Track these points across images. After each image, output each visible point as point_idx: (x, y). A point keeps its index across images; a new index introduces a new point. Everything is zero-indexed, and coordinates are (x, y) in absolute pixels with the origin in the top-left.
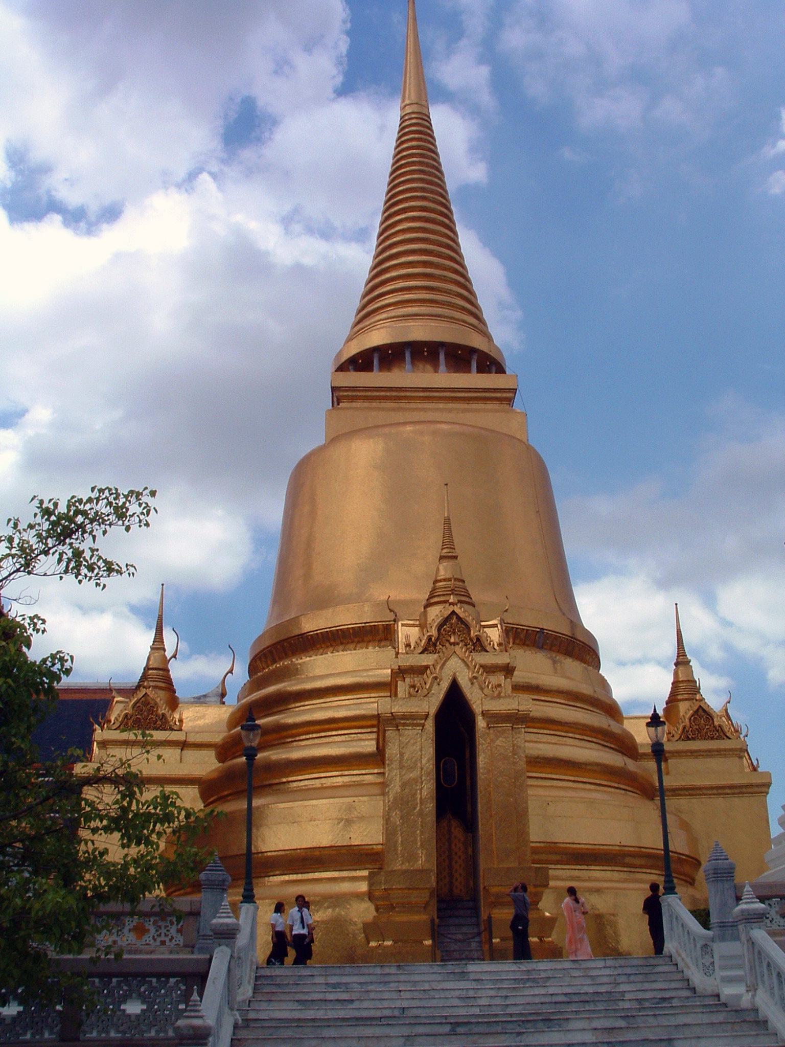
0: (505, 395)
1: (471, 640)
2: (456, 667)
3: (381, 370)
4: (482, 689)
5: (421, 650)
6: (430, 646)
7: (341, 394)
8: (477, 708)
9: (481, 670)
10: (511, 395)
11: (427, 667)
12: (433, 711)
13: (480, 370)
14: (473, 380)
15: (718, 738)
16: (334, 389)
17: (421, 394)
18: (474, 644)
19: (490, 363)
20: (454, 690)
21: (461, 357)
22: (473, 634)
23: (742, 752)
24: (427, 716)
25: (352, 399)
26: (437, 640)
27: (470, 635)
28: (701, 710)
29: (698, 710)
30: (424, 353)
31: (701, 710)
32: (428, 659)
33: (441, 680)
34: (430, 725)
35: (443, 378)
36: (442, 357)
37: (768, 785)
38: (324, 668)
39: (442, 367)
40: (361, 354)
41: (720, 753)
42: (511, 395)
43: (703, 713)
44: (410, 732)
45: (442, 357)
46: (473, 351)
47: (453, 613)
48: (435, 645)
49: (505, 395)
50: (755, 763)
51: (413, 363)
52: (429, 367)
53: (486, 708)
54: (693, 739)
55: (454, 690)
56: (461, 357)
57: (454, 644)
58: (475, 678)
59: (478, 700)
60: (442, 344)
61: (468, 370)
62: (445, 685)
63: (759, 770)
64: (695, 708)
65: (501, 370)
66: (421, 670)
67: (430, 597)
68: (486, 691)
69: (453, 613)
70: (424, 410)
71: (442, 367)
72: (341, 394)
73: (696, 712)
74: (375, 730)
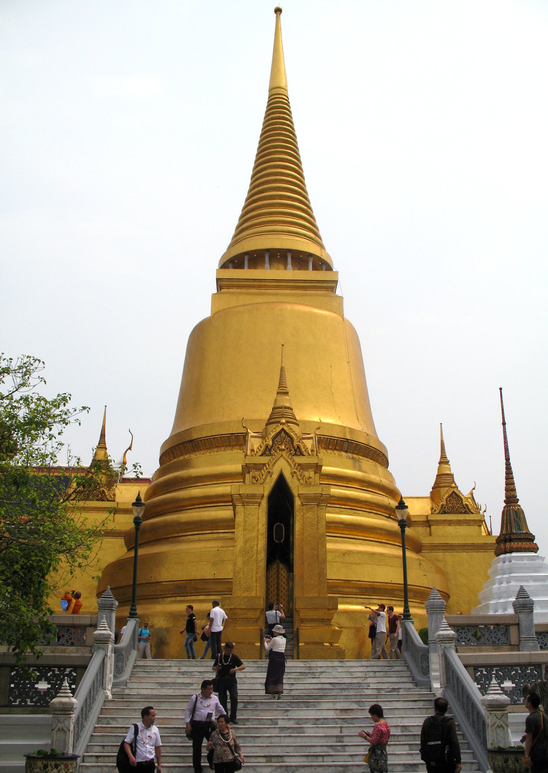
1: (294, 447)
2: (282, 465)
3: (249, 268)
4: (299, 480)
5: (260, 453)
6: (267, 451)
7: (222, 283)
8: (295, 492)
9: (299, 467)
10: (334, 285)
11: (264, 465)
12: (266, 493)
13: (315, 268)
14: (310, 274)
16: (218, 280)
17: (274, 284)
18: (295, 450)
20: (281, 479)
24: (263, 496)
25: (229, 287)
26: (272, 447)
27: (293, 444)
32: (264, 460)
33: (272, 473)
34: (264, 503)
35: (290, 273)
39: (290, 266)
40: (236, 257)
42: (334, 285)
44: (252, 508)
47: (283, 429)
48: (270, 450)
49: (329, 285)
51: (270, 264)
52: (281, 266)
53: (300, 492)
55: (281, 479)
56: (301, 259)
58: (295, 473)
60: (290, 251)
61: (307, 269)
62: (275, 476)
65: (329, 268)
66: (259, 467)
67: (270, 419)
68: (301, 481)
69: (283, 429)
70: (276, 294)
71: (290, 266)
72: (222, 283)
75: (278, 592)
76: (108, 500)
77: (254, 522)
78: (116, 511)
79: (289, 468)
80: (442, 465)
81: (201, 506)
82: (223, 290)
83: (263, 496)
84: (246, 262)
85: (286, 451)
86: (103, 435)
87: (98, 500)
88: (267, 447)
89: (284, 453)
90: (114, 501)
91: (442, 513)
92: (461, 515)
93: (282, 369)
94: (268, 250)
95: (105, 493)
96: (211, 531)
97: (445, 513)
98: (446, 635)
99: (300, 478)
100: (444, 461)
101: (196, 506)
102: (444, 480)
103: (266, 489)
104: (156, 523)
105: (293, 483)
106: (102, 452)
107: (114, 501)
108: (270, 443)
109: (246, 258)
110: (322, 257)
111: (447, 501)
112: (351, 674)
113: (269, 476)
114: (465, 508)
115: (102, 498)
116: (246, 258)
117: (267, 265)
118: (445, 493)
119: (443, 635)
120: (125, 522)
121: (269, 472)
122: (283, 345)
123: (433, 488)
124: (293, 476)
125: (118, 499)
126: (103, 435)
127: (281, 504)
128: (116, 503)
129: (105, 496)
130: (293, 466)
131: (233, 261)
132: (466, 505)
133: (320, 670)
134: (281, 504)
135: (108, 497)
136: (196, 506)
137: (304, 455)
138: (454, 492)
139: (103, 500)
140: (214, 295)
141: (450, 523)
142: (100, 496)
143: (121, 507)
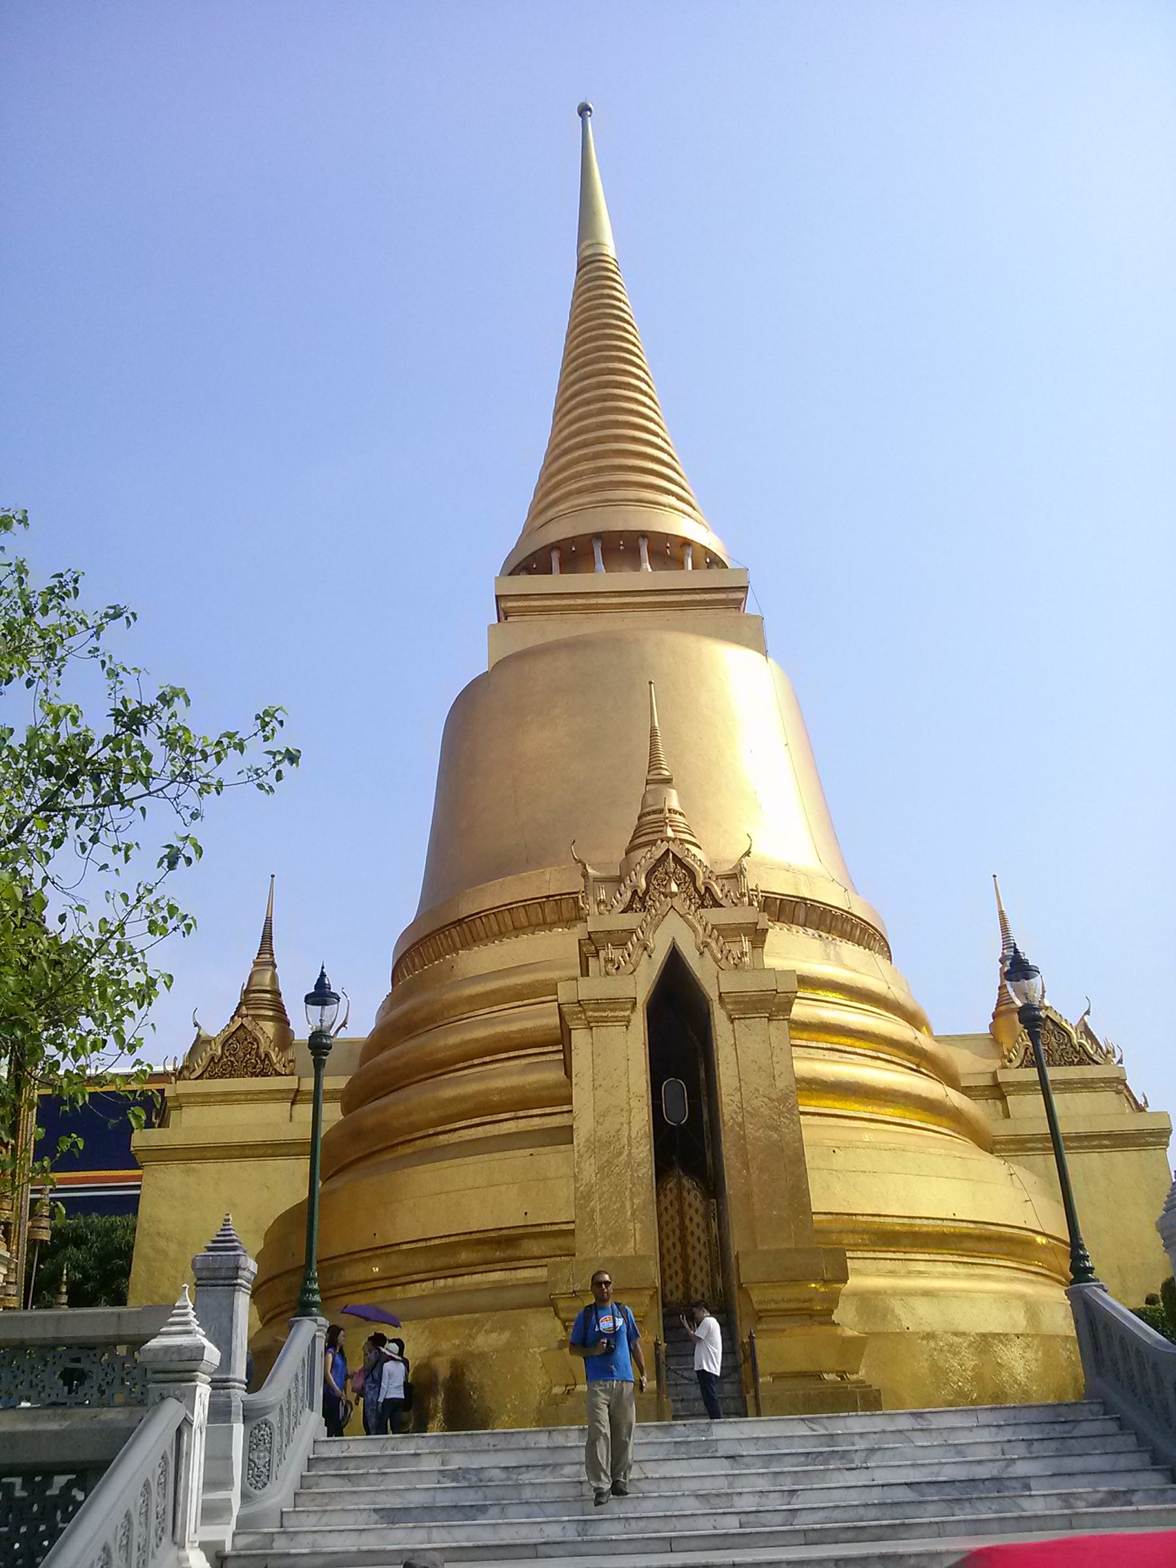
1: (696, 890)
2: (674, 930)
4: (717, 961)
7: (509, 604)
11: (632, 932)
15: (1081, 1063)
18: (702, 897)
20: (675, 960)
23: (1118, 1085)
25: (524, 612)
34: (639, 1021)
37: (1167, 1132)
38: (483, 961)
41: (1088, 1085)
42: (740, 595)
48: (642, 900)
50: (1141, 1101)
55: (675, 960)
62: (660, 956)
63: (1148, 1110)
66: (620, 939)
67: (634, 838)
68: (723, 964)
72: (509, 604)
74: (561, 1047)
75: (684, 1247)
77: (615, 1071)
81: (487, 1059)
82: (509, 619)
84: (555, 564)
86: (267, 938)
87: (254, 1075)
88: (635, 892)
89: (676, 902)
94: (598, 536)
96: (512, 1115)
101: (476, 1061)
103: (642, 982)
105: (702, 969)
109: (555, 556)
112: (959, 1453)
115: (263, 1068)
116: (555, 556)
117: (600, 566)
126: (267, 938)
127: (679, 1022)
129: (271, 1064)
130: (700, 929)
131: (530, 563)
133: (861, 1444)
134: (679, 1022)
135: (278, 1067)
136: (476, 1061)
137: (722, 906)
139: (266, 1075)
142: (260, 1065)
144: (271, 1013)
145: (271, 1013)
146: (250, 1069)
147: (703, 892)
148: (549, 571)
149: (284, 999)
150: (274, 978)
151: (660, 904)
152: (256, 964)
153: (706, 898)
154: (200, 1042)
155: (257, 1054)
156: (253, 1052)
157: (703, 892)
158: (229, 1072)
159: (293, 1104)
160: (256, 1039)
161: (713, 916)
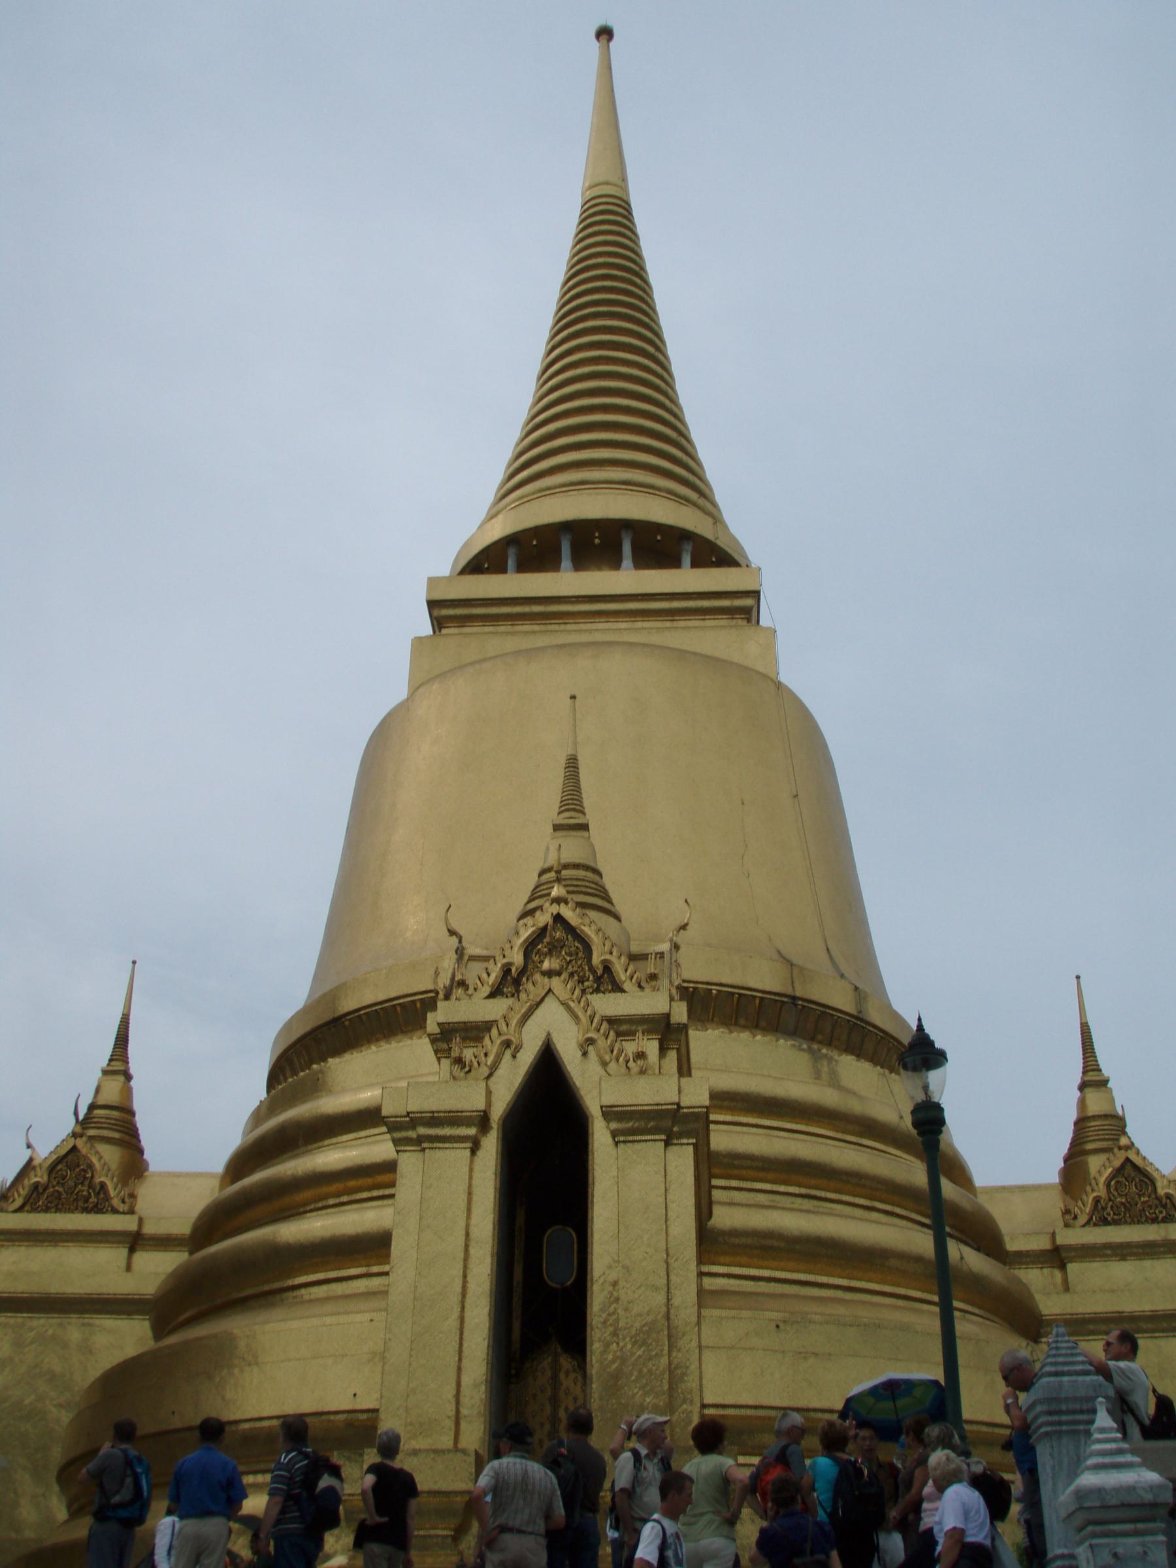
0: (738, 603)
1: (592, 970)
2: (555, 1021)
4: (604, 1064)
5: (486, 990)
8: (593, 1107)
9: (605, 1025)
16: (432, 604)
18: (598, 979)
19: (715, 554)
20: (548, 1063)
21: (658, 546)
22: (596, 960)
24: (483, 1121)
26: (523, 971)
28: (1128, 1169)
29: (1122, 1166)
30: (594, 542)
31: (1128, 1169)
33: (518, 1048)
34: (491, 1144)
36: (627, 549)
42: (749, 602)
43: (1134, 1174)
45: (627, 549)
46: (685, 535)
48: (517, 983)
49: (738, 603)
53: (608, 1100)
54: (1116, 1222)
55: (548, 1060)
56: (658, 546)
57: (549, 974)
58: (591, 1041)
59: (596, 1085)
62: (528, 1056)
64: (1117, 1163)
68: (613, 1066)
69: (558, 918)
71: (627, 562)
73: (1119, 1171)
76: (115, 1211)
78: (135, 1241)
79: (574, 1028)
80: (1087, 1090)
81: (345, 1199)
82: (444, 631)
83: (483, 1121)
84: (511, 563)
85: (565, 975)
88: (507, 970)
89: (556, 983)
90: (132, 1212)
91: (1095, 1225)
92: (1154, 1227)
93: (572, 764)
94: (567, 526)
95: (106, 1193)
97: (1105, 1222)
98: (1118, 1490)
99: (607, 1058)
100: (1093, 1079)
101: (331, 1201)
102: (1098, 1130)
104: (214, 1256)
106: (116, 1083)
107: (132, 1212)
108: (517, 959)
110: (719, 543)
111: (1108, 1186)
113: (508, 1053)
114: (1164, 1206)
115: (99, 1203)
117: (566, 563)
118: (1099, 1167)
119: (1099, 1491)
120: (154, 1270)
121: (507, 1044)
122: (573, 697)
123: (1067, 1160)
124: (585, 1054)
125: (141, 1206)
128: (135, 1218)
129: (108, 1198)
130: (584, 1019)
132: (1168, 1196)
135: (116, 1202)
137: (624, 991)
138: (1128, 1160)
140: (418, 643)
141: (1122, 1251)
142: (93, 1199)
143: (148, 1229)
144: (116, 1135)
145: (116, 1135)
146: (81, 1204)
147: (599, 973)
148: (503, 570)
149: (141, 1121)
150: (127, 1092)
151: (533, 988)
152: (105, 1072)
153: (606, 980)
154: (29, 1166)
155: (91, 1186)
156: (87, 1183)
157: (599, 973)
158: (57, 1204)
159: (132, 1250)
160: (91, 1166)
161: (608, 1004)
